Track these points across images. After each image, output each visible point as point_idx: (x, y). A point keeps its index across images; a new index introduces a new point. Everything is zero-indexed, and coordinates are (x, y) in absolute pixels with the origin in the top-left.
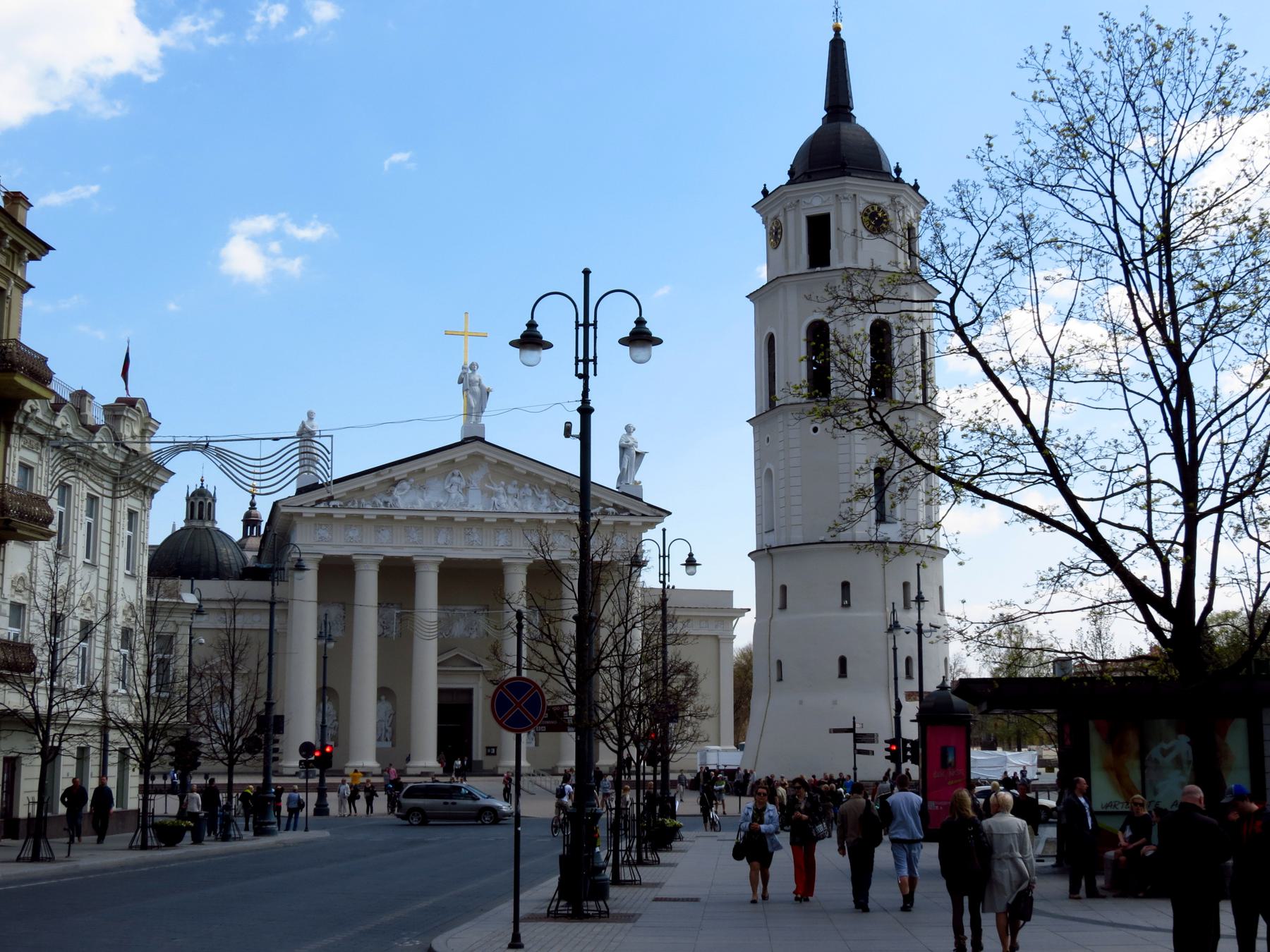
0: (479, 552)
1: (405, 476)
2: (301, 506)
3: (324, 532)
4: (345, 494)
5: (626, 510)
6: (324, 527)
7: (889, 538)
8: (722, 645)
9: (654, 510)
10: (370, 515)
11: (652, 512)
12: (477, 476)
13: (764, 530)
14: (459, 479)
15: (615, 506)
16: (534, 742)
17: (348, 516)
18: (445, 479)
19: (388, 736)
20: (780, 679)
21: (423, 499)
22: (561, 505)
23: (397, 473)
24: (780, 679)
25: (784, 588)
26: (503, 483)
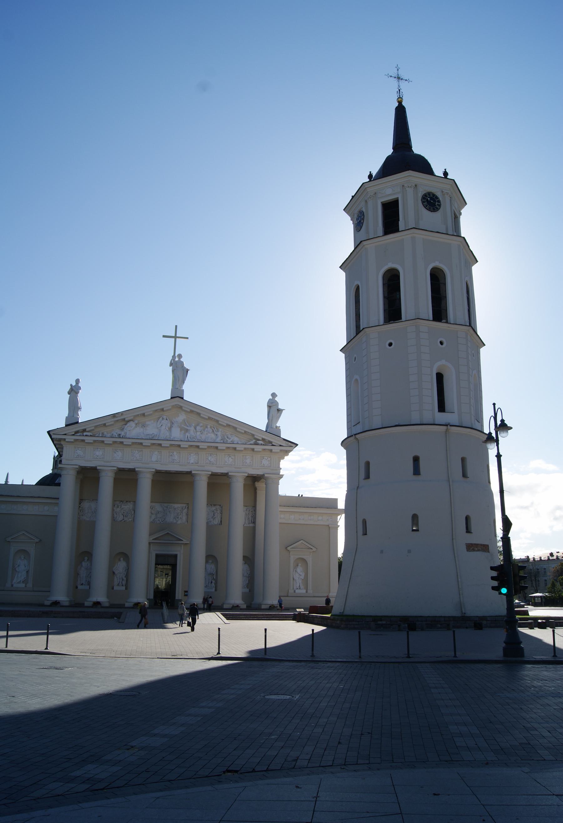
1: (132, 418)
2: (65, 434)
5: (270, 442)
6: (80, 449)
7: (450, 423)
9: (287, 442)
13: (353, 425)
15: (263, 440)
16: (214, 589)
17: (95, 441)
18: (157, 421)
19: (124, 583)
20: (365, 534)
22: (230, 439)
24: (365, 534)
25: (368, 464)
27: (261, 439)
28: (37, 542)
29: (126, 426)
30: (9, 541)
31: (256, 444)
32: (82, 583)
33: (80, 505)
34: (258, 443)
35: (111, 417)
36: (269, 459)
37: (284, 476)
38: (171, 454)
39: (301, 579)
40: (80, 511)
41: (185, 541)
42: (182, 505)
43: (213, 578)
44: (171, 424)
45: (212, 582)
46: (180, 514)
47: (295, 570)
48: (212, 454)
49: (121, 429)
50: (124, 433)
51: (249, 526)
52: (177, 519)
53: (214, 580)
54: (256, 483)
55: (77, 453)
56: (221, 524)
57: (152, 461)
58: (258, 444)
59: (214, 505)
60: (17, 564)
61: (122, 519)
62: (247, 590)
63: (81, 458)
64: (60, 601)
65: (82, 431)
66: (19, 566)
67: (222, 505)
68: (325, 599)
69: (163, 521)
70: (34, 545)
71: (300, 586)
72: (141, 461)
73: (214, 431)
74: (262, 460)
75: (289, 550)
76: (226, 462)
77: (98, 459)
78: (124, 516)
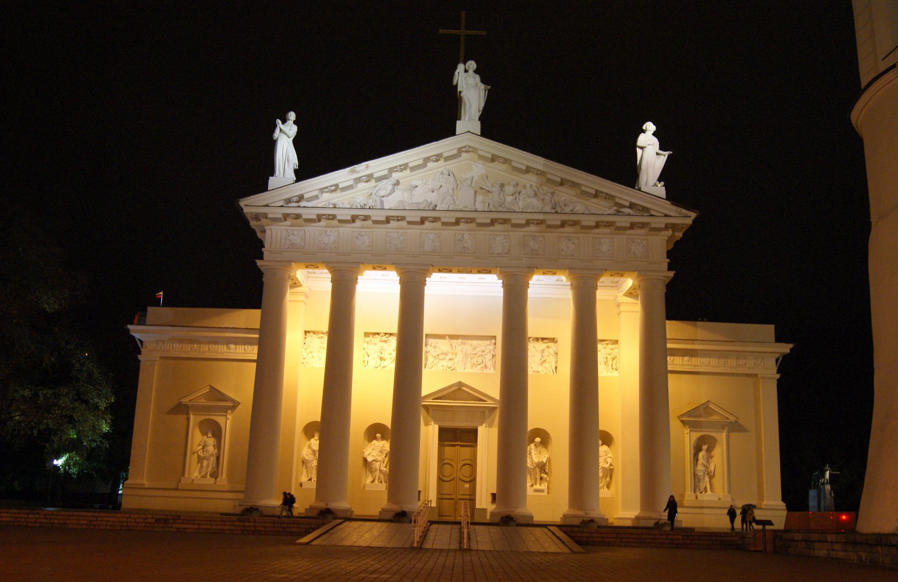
2: (267, 206)
15: (632, 206)
27: (628, 204)
31: (618, 213)
34: (624, 212)
35: (349, 172)
36: (644, 243)
38: (459, 238)
50: (373, 202)
55: (290, 240)
60: (200, 445)
64: (259, 508)
72: (404, 251)
73: (539, 193)
76: (562, 250)
77: (327, 249)
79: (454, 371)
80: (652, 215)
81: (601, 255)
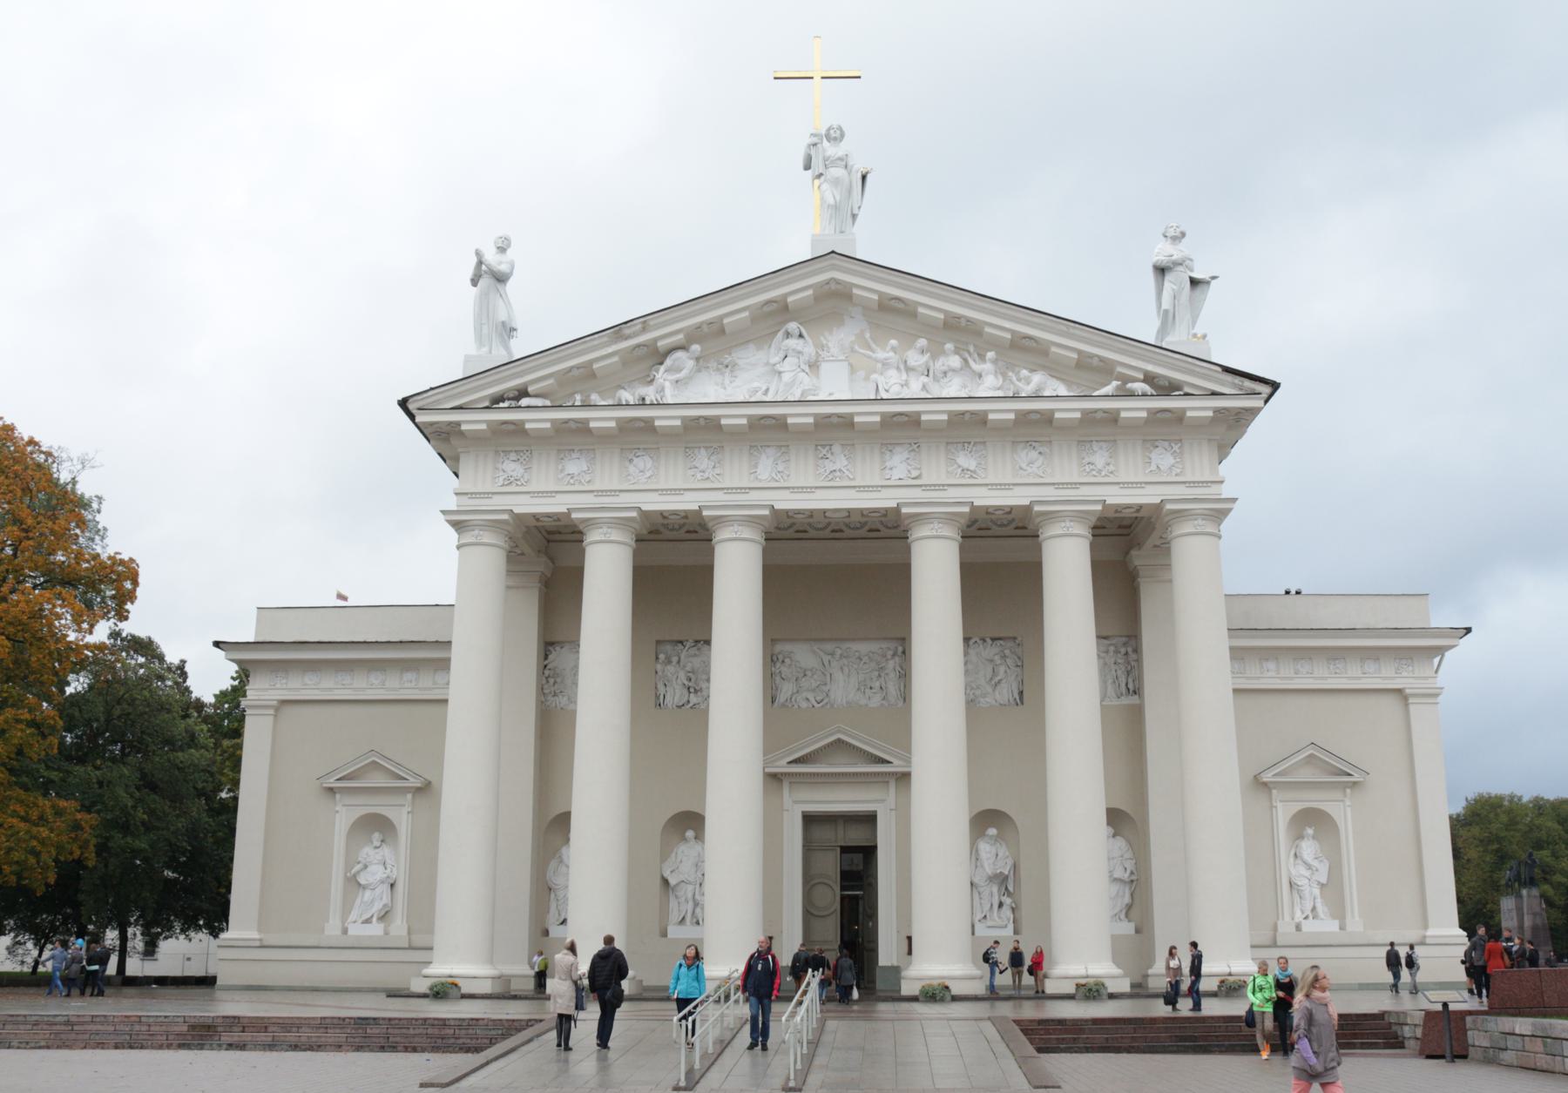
0: (852, 493)
3: (513, 466)
4: (551, 381)
6: (513, 456)
8: (1412, 708)
9: (1238, 380)
10: (602, 420)
11: (1234, 386)
12: (839, 339)
14: (801, 341)
15: (1149, 379)
16: (1011, 926)
18: (770, 346)
21: (725, 388)
23: (662, 334)
26: (893, 342)
27: (1141, 377)
28: (418, 790)
29: (662, 368)
30: (331, 790)
32: (562, 920)
33: (546, 662)
37: (1236, 506)
39: (1319, 883)
40: (548, 682)
41: (897, 766)
42: (884, 645)
43: (1006, 889)
44: (817, 352)
45: (1001, 905)
46: (880, 676)
47: (1292, 853)
48: (969, 443)
49: (649, 379)
51: (1118, 703)
52: (868, 690)
53: (1008, 896)
54: (1134, 553)
55: (504, 471)
56: (1022, 703)
57: (760, 481)
58: (1131, 395)
59: (993, 639)
60: (359, 863)
61: (685, 699)
62: (1127, 928)
63: (517, 485)
65: (516, 393)
66: (366, 867)
67: (1020, 639)
68: (1383, 952)
69: (822, 701)
70: (409, 796)
71: (1314, 909)
74: (1151, 452)
75: (1265, 784)
76: (1021, 468)
78: (692, 690)
79: (828, 706)
80: (1187, 394)
81: (1094, 473)
